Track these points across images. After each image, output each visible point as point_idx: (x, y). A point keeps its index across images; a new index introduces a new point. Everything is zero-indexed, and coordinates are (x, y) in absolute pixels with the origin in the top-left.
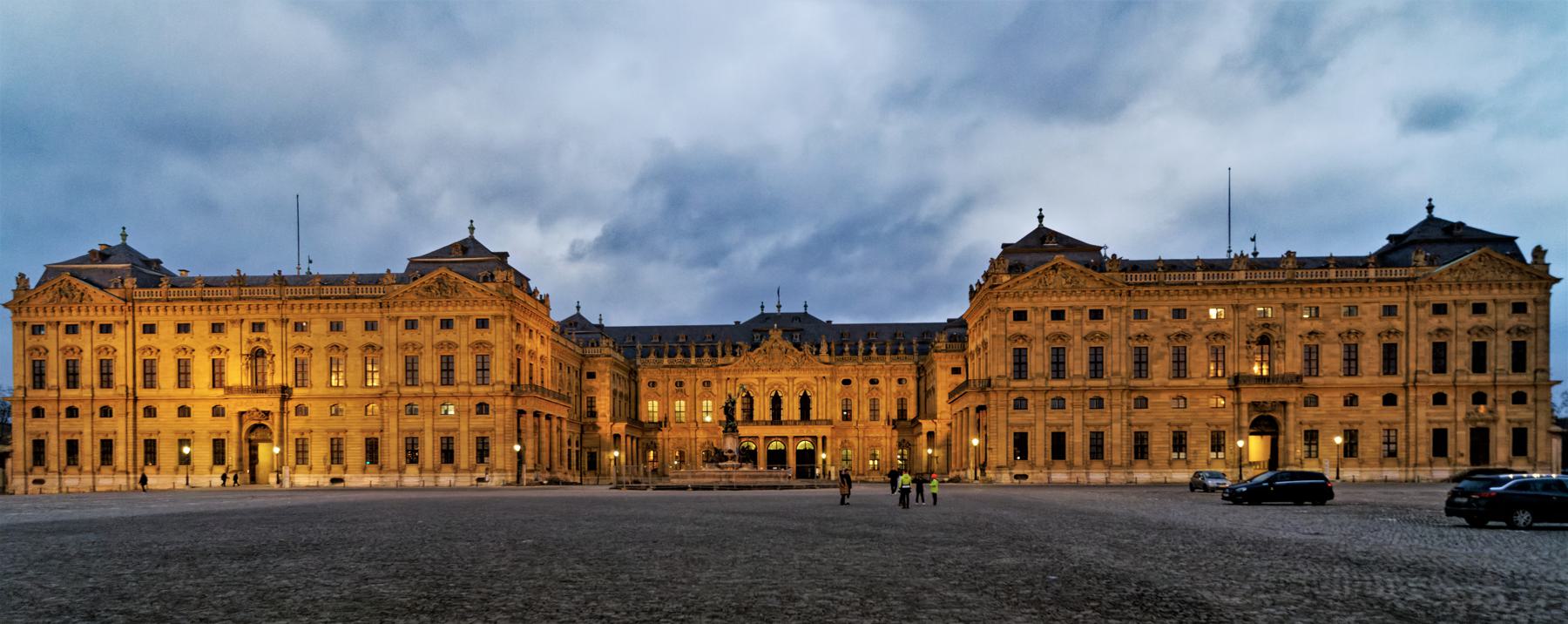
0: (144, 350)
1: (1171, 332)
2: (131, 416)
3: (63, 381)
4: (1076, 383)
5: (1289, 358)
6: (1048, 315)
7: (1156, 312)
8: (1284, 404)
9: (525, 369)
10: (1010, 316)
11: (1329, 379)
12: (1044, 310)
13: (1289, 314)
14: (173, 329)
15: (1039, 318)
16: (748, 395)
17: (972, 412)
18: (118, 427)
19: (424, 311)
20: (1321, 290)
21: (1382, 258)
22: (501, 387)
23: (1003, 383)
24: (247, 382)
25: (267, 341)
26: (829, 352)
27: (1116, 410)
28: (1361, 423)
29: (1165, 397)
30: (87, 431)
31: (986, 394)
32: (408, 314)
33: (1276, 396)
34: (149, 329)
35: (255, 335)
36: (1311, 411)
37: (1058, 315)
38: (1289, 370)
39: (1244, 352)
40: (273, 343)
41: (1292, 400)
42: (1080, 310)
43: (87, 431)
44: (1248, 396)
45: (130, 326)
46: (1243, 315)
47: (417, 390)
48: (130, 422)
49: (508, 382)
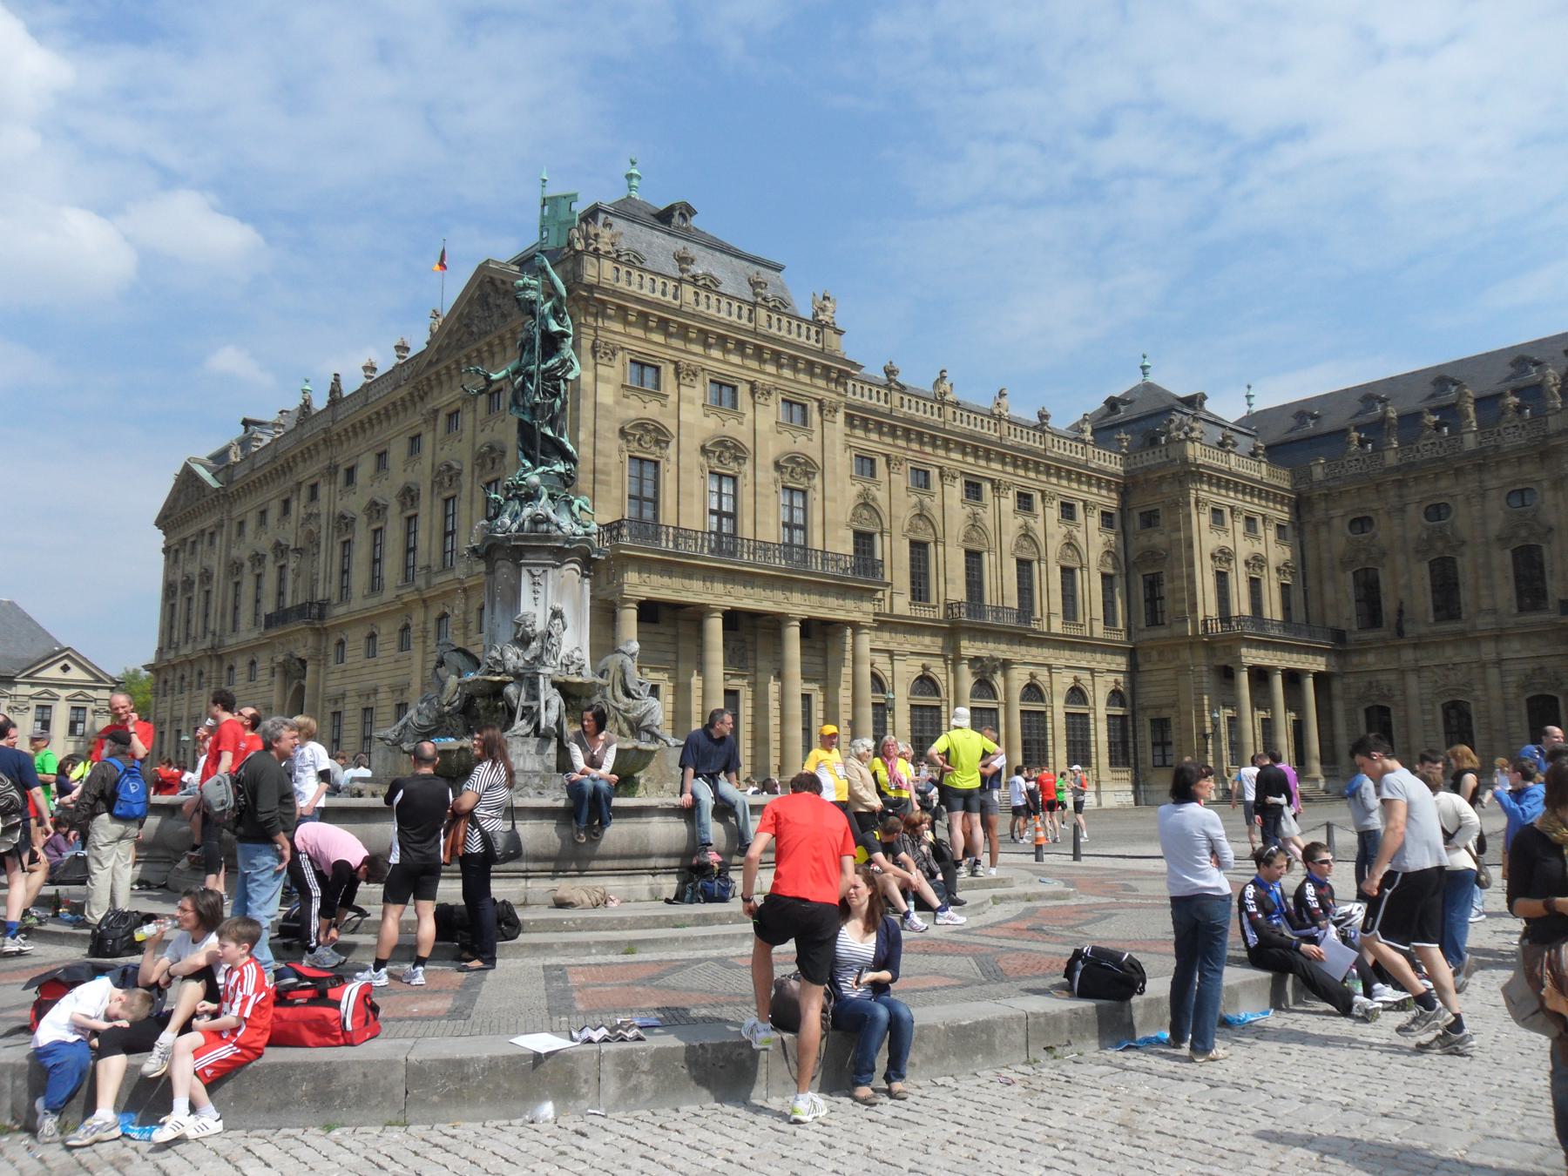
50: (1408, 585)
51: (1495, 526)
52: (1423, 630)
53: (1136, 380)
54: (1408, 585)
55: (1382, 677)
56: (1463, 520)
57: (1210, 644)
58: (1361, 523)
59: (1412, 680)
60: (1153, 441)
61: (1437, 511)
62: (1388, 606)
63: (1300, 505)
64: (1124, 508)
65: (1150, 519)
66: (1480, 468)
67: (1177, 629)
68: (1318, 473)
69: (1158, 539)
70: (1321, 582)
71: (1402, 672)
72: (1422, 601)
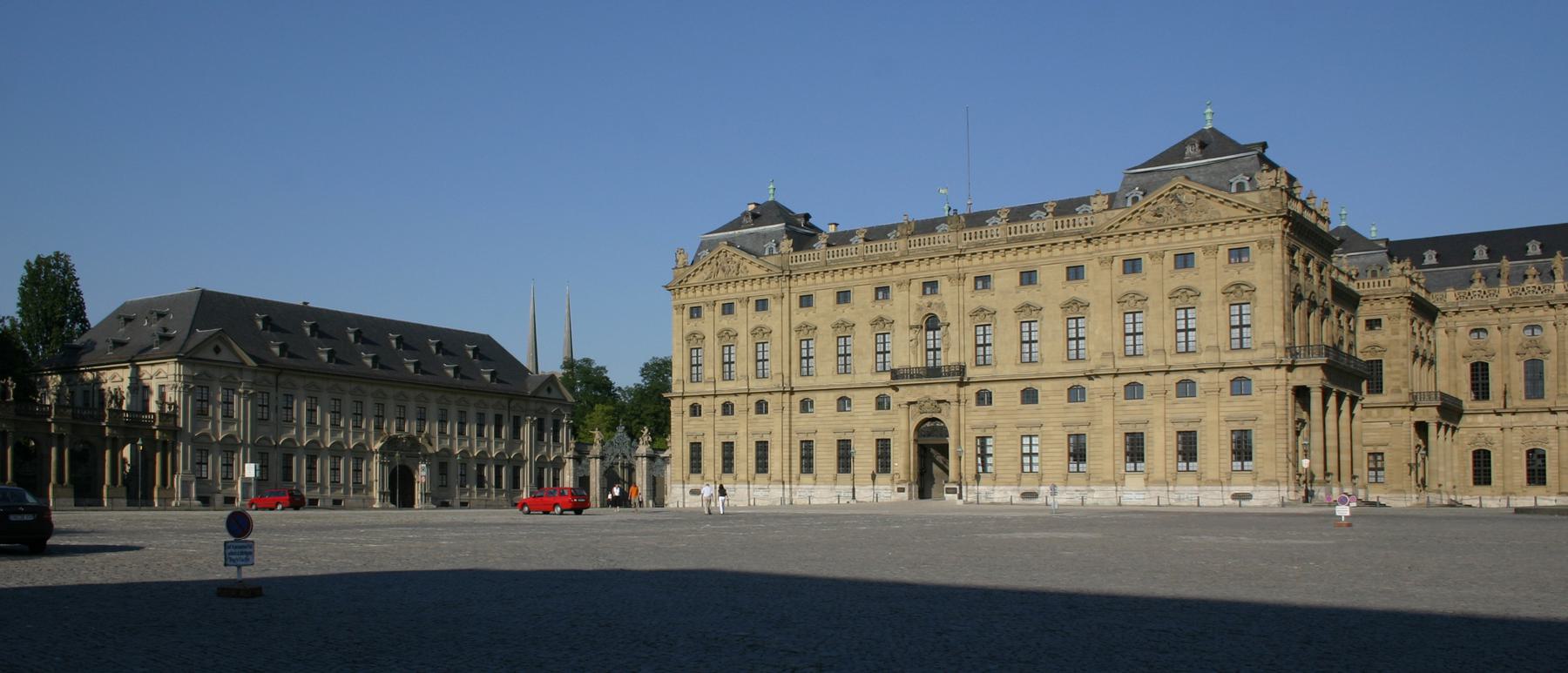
0: (799, 329)
2: (786, 412)
3: (718, 372)
14: (832, 299)
18: (773, 426)
22: (1270, 352)
24: (917, 361)
25: (941, 306)
30: (742, 431)
32: (1127, 249)
34: (806, 301)
35: (926, 300)
40: (948, 308)
43: (742, 431)
45: (786, 300)
48: (786, 420)
49: (1280, 343)
55: (1486, 431)
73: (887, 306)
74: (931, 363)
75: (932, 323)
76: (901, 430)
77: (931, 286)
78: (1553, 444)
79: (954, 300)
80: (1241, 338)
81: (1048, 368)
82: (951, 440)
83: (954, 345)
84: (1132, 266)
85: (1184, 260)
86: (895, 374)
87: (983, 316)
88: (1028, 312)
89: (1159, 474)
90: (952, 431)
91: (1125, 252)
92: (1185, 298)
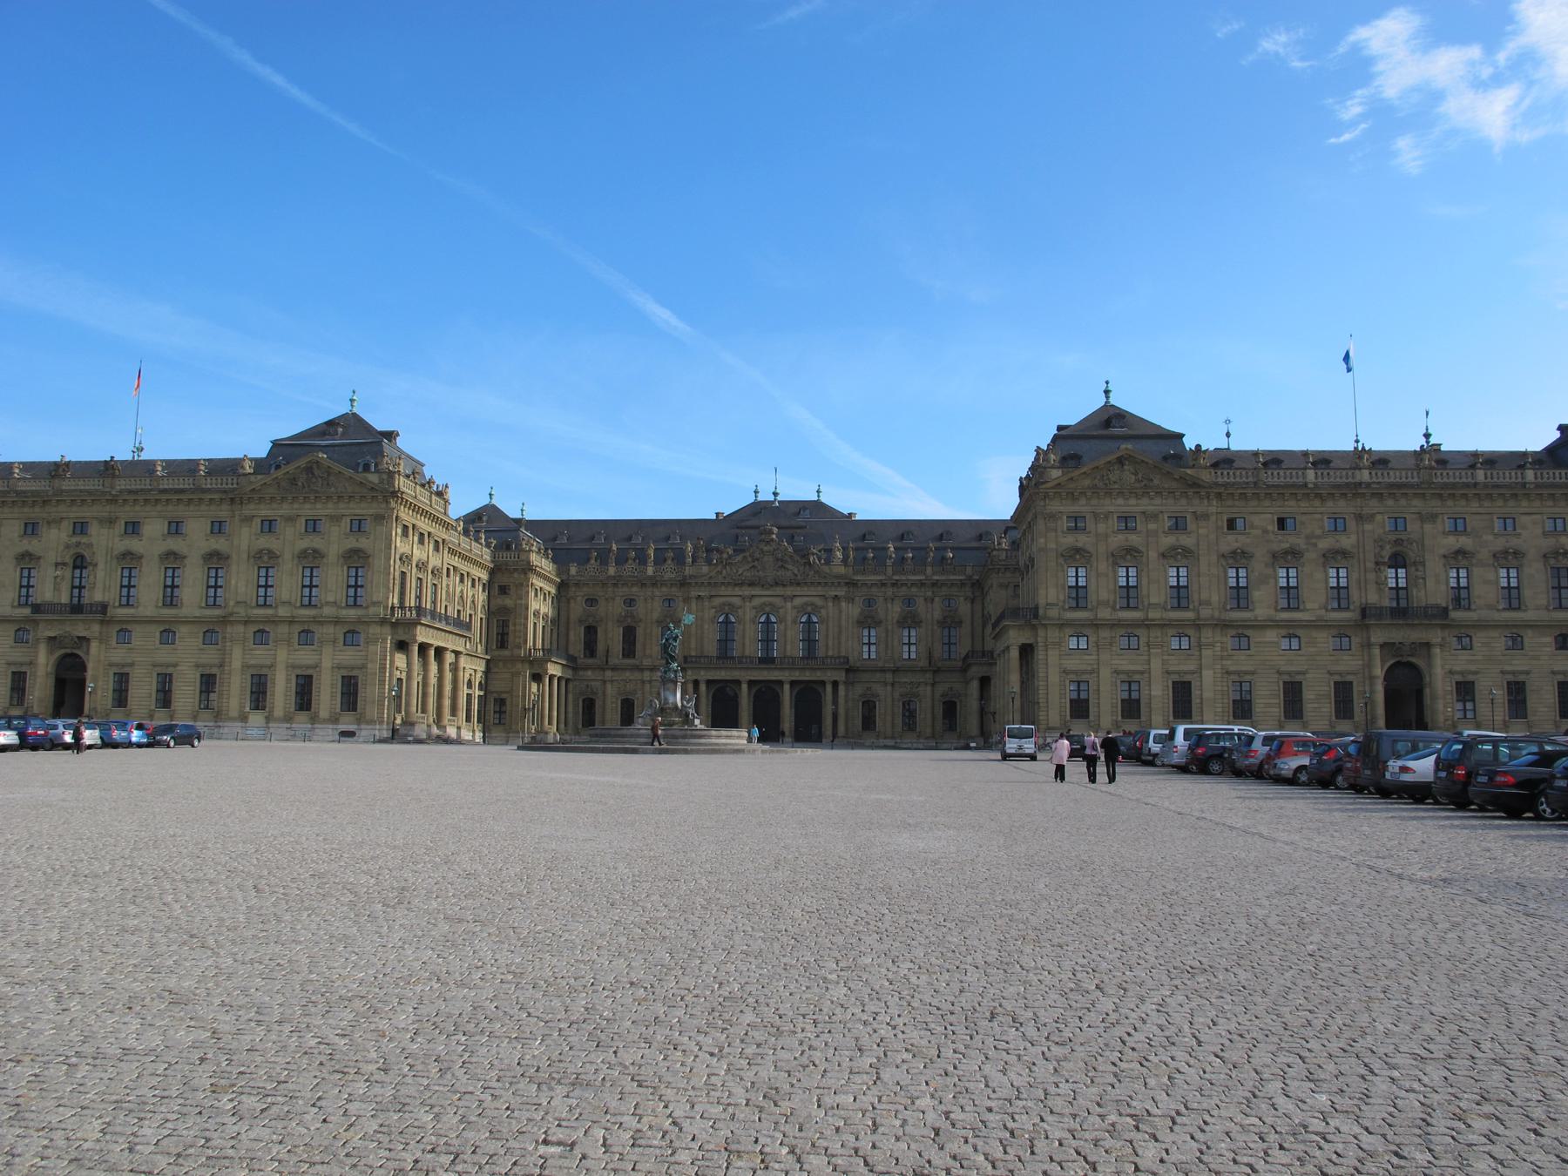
1: (1276, 547)
4: (1151, 615)
5: (1430, 583)
6: (1114, 523)
7: (1256, 520)
8: (1428, 645)
9: (412, 584)
10: (1064, 523)
11: (1484, 614)
12: (1107, 516)
13: (1428, 527)
15: (1102, 527)
16: (727, 622)
17: (1014, 653)
19: (285, 510)
20: (1465, 496)
21: (1552, 454)
23: (1053, 613)
26: (845, 560)
27: (1207, 653)
28: (1527, 673)
29: (1271, 635)
31: (1034, 628)
33: (1416, 636)
36: (1464, 656)
37: (1126, 520)
38: (1432, 601)
39: (1371, 576)
41: (1434, 641)
42: (1154, 517)
44: (1378, 637)
46: (1368, 527)
47: (270, 611)
50: (611, 638)
51: (656, 615)
52: (616, 661)
53: (486, 501)
54: (611, 638)
56: (640, 609)
57: (530, 661)
58: (592, 601)
59: (609, 686)
60: (508, 547)
61: (630, 602)
62: (601, 647)
63: (562, 587)
64: (490, 581)
65: (503, 590)
66: (654, 585)
67: (516, 652)
68: (573, 570)
69: (508, 602)
70: (568, 629)
71: (605, 682)
72: (617, 646)
73: (35, 542)
74: (75, 600)
75: (80, 563)
76: (44, 663)
77: (80, 527)
78: (639, 695)
79: (104, 541)
80: (356, 596)
81: (185, 612)
82: (89, 674)
83: (99, 585)
84: (269, 526)
85: (313, 526)
86: (37, 608)
87: (129, 560)
88: (172, 559)
89: (279, 712)
90: (90, 666)
91: (263, 513)
92: (311, 559)
